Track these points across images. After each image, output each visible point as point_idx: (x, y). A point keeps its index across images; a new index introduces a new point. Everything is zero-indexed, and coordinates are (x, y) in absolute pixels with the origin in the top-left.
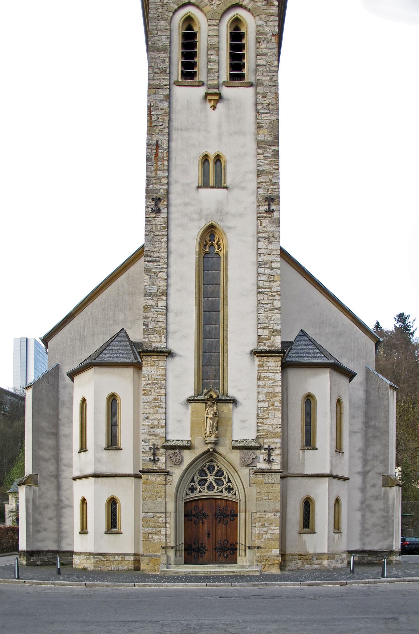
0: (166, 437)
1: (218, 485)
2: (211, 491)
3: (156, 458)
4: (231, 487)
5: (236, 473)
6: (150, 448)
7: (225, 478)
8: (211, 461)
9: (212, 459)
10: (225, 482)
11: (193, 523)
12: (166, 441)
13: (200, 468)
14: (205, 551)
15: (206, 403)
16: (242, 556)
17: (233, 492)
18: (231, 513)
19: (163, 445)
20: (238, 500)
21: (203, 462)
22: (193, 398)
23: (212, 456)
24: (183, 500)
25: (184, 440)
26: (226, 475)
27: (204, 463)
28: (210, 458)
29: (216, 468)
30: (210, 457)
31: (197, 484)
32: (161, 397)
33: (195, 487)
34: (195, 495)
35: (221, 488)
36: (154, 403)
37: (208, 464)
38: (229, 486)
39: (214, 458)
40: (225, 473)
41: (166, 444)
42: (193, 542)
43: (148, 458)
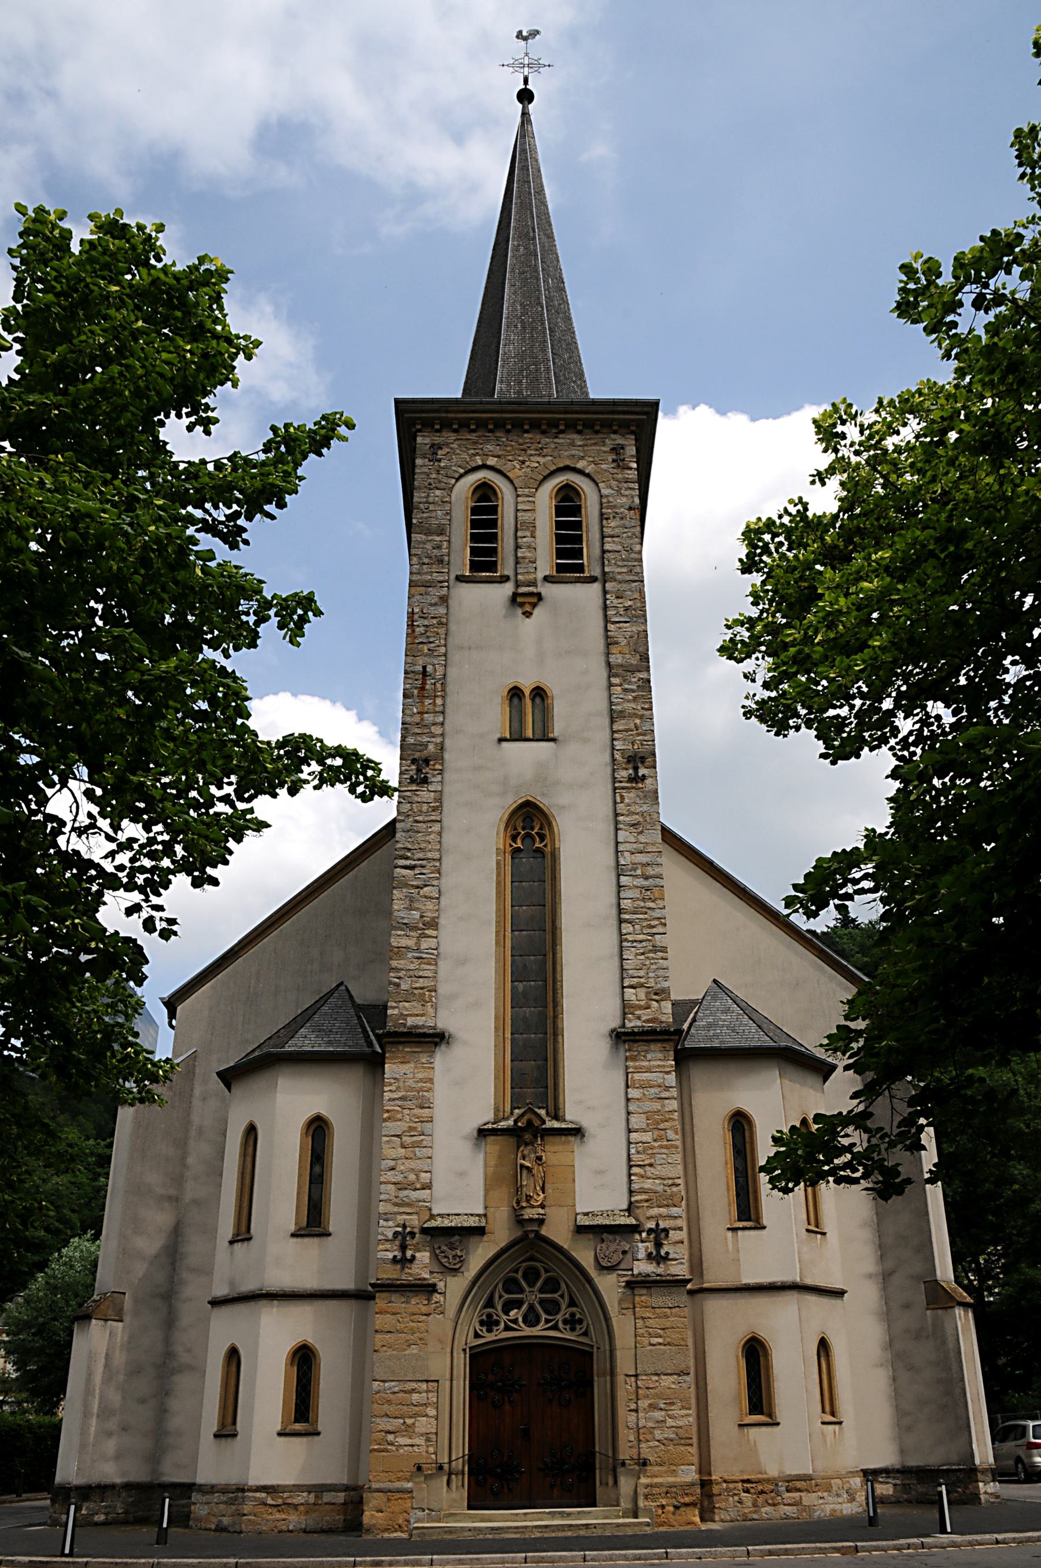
0: (430, 1210)
1: (547, 1312)
3: (409, 1254)
5: (587, 1286)
6: (396, 1233)
8: (531, 1258)
10: (563, 1307)
12: (432, 1217)
15: (519, 1137)
16: (607, 1484)
19: (426, 1225)
22: (490, 1126)
25: (472, 1215)
29: (544, 1276)
38: (573, 1315)
40: (563, 1286)
41: (433, 1224)
43: (390, 1255)
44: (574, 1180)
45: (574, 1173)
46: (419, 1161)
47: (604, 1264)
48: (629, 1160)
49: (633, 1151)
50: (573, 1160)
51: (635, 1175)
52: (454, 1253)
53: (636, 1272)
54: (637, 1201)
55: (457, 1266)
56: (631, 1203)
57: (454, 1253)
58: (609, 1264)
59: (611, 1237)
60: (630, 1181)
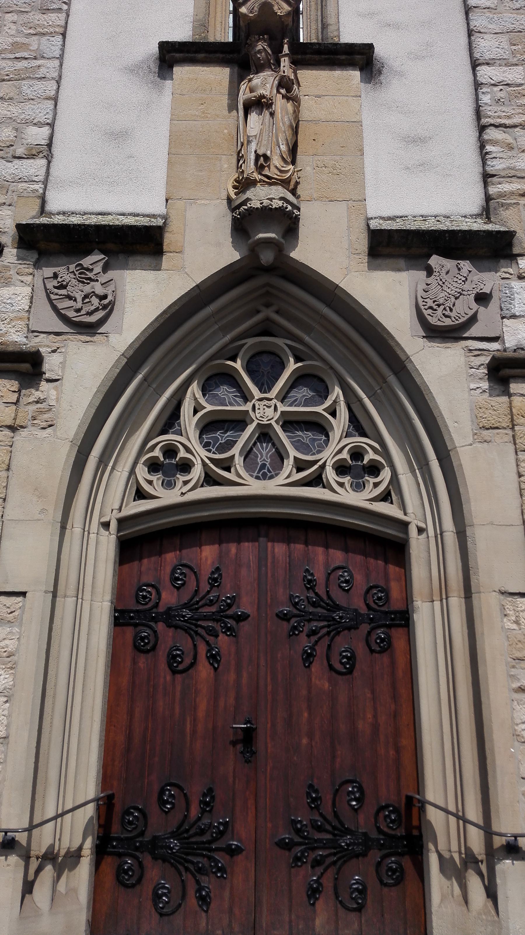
2: (264, 477)
4: (370, 456)
7: (334, 414)
9: (268, 319)
11: (163, 665)
13: (212, 358)
14: (222, 859)
17: (376, 485)
18: (368, 605)
20: (405, 525)
21: (225, 329)
23: (268, 305)
24: (114, 525)
26: (342, 398)
27: (228, 338)
28: (258, 312)
30: (263, 308)
31: (193, 441)
32: (44, 39)
33: (182, 454)
34: (183, 494)
35: (316, 462)
36: (10, 63)
37: (250, 341)
39: (277, 312)
42: (156, 788)
44: (361, 151)
45: (360, 135)
46: (28, 106)
47: (433, 321)
48: (478, 113)
49: (485, 99)
50: (359, 112)
51: (495, 143)
52: (87, 289)
53: (510, 342)
54: (502, 195)
55: (93, 319)
56: (488, 198)
57: (87, 289)
58: (448, 322)
59: (449, 264)
60: (484, 156)
